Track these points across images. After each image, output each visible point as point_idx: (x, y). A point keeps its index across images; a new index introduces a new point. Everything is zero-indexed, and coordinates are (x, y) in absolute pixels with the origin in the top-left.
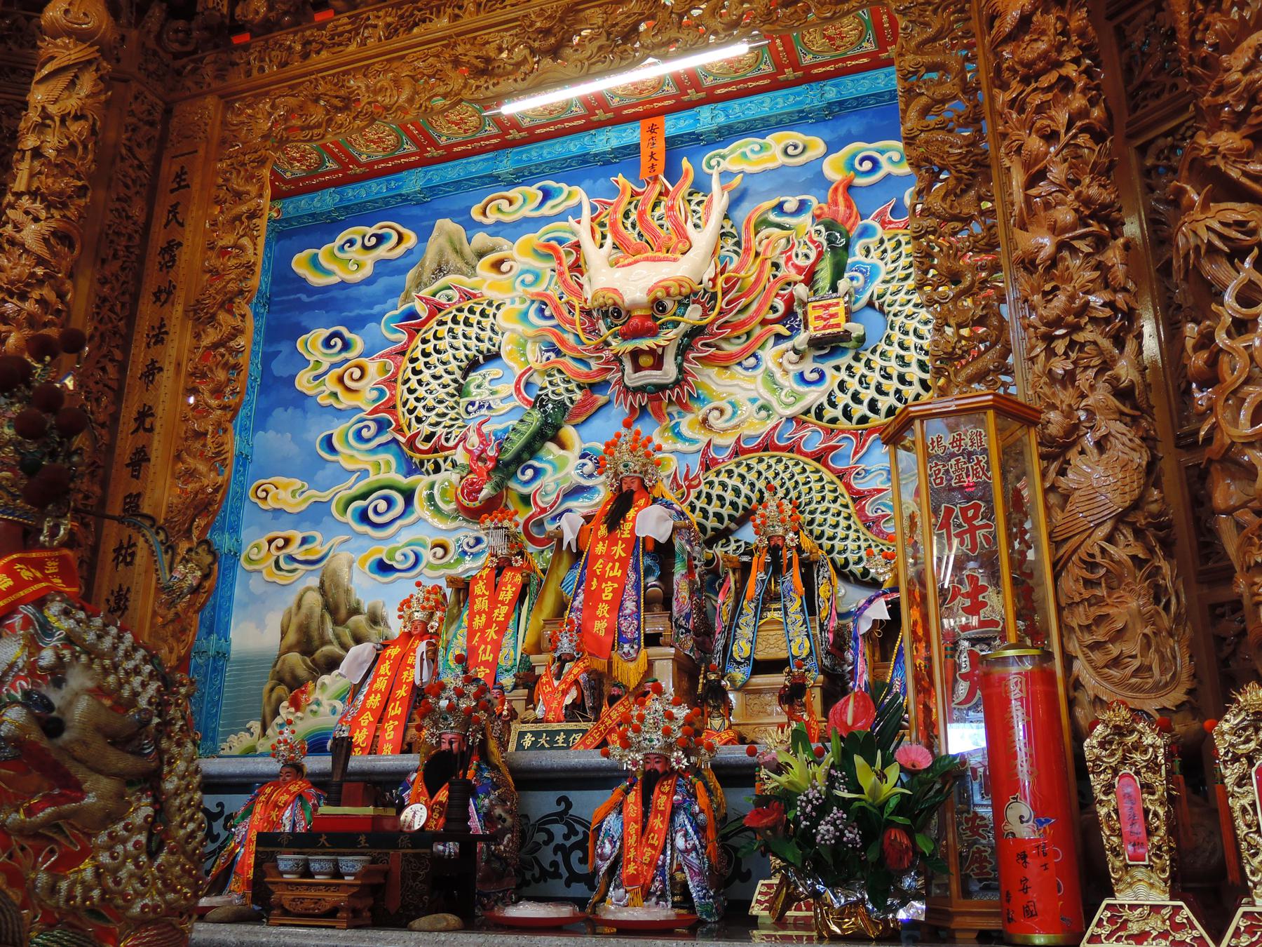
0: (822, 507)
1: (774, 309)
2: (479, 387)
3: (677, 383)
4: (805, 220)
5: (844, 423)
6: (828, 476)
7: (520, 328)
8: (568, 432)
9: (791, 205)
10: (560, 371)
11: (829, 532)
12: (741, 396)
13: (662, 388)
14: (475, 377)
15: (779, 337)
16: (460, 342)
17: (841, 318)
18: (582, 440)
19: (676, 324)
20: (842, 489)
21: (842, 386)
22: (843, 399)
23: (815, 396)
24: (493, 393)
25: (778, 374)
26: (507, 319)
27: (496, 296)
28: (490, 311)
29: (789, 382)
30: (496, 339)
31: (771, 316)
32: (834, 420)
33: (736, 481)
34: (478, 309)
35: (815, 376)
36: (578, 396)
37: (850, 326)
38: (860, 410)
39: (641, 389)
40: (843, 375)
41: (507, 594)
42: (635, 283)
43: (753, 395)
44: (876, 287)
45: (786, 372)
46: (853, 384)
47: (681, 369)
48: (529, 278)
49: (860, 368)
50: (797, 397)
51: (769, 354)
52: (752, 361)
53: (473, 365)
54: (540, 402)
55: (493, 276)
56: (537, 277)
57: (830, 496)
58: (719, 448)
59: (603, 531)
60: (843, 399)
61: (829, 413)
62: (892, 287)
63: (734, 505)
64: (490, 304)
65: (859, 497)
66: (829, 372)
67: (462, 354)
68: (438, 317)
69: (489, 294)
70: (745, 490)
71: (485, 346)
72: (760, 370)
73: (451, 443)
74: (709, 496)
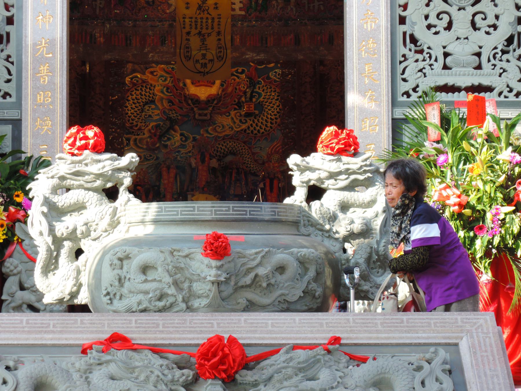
0: (245, 156)
1: (235, 101)
2: (148, 110)
3: (210, 119)
4: (243, 76)
5: (251, 134)
6: (246, 148)
7: (162, 95)
8: (177, 127)
9: (240, 70)
10: (174, 110)
11: (247, 162)
12: (225, 123)
13: (206, 120)
14: (147, 107)
15: (235, 109)
16: (144, 97)
17: (253, 109)
18: (181, 130)
19: (211, 106)
20: (250, 151)
21: (251, 125)
22: (252, 129)
23: (244, 126)
24: (152, 113)
25: (235, 119)
26: (158, 91)
27: (153, 83)
28: (152, 88)
29: (237, 122)
30: (154, 97)
31: (234, 103)
32: (249, 133)
33: (223, 147)
34: (148, 87)
35: (244, 121)
36: (179, 118)
37: (255, 111)
38: (256, 132)
39: (200, 120)
40: (251, 122)
41: (172, 175)
42: (203, 93)
43: (228, 124)
44: (261, 99)
45: (237, 119)
46: (254, 125)
47: (211, 116)
48: (163, 79)
49: (256, 121)
50: (240, 126)
51: (233, 113)
52: (228, 114)
53: (146, 103)
54: (169, 119)
55: (150, 76)
56: (166, 80)
57: (247, 153)
58: (219, 137)
59: (200, 163)
60: (252, 129)
61: (248, 131)
62: (265, 100)
63: (223, 153)
64: (151, 85)
65: (254, 154)
66: (248, 121)
67: (144, 100)
68: (135, 87)
69: (150, 82)
70: (226, 150)
71: (151, 99)
72: (229, 117)
73: (143, 128)
74: (217, 151)
